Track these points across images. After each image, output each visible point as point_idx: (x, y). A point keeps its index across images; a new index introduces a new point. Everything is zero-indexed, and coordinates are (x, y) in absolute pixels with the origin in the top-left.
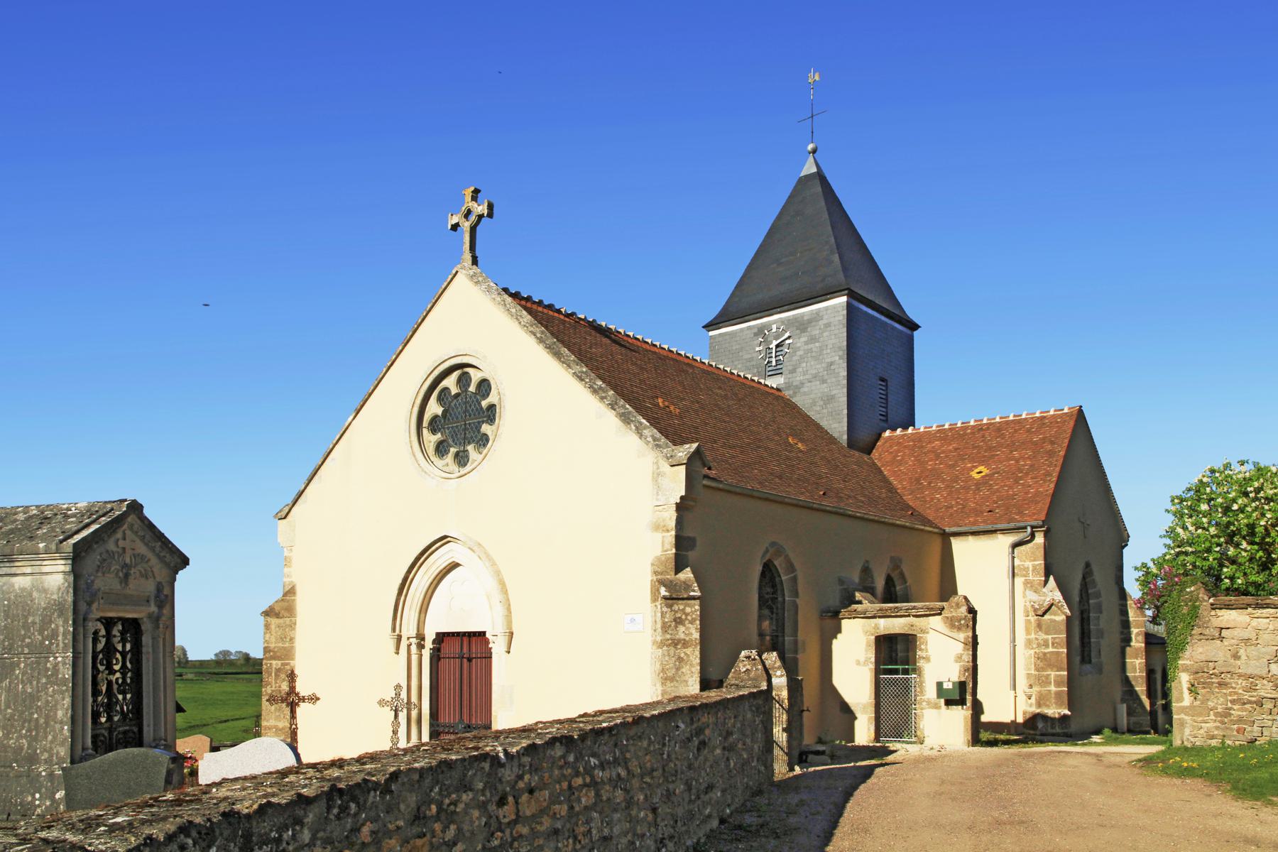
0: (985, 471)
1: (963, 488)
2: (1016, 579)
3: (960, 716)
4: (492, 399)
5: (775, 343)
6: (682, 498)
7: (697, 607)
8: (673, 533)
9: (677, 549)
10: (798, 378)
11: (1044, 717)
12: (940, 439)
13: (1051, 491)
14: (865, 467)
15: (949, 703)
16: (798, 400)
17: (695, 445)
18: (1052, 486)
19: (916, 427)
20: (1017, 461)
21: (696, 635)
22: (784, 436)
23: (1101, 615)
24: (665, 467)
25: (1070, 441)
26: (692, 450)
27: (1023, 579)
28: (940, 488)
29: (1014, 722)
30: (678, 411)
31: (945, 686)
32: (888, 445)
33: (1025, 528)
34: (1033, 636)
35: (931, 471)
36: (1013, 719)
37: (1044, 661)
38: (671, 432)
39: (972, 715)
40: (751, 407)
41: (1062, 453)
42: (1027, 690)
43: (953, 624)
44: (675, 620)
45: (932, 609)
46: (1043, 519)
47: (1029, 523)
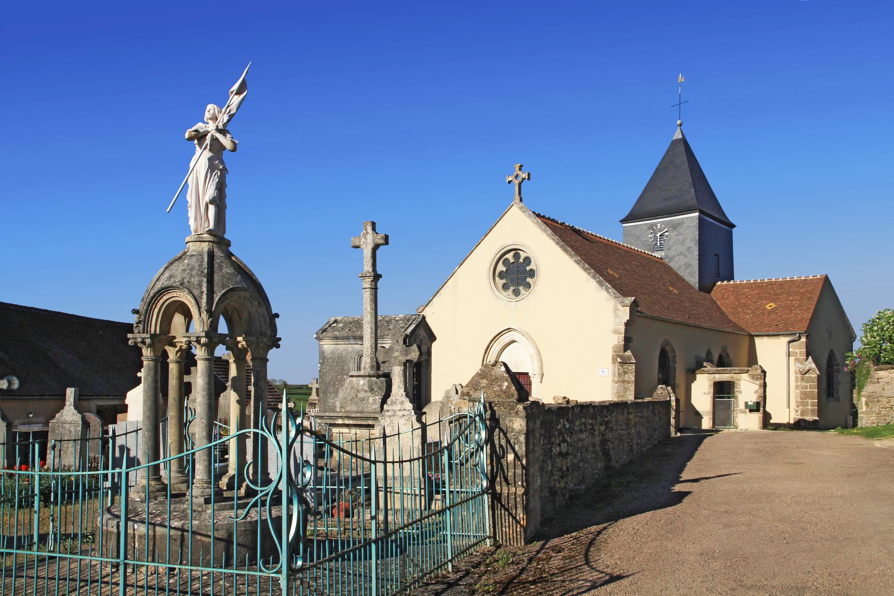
0: (774, 305)
1: (761, 313)
2: (790, 358)
3: (757, 417)
4: (532, 266)
5: (659, 234)
6: (627, 320)
7: (634, 367)
8: (623, 335)
9: (625, 342)
10: (672, 254)
11: (804, 421)
12: (748, 288)
13: (810, 317)
14: (708, 301)
15: (751, 411)
16: (672, 265)
17: (633, 298)
18: (810, 315)
19: (735, 281)
20: (792, 301)
21: (633, 379)
22: (667, 286)
23: (839, 375)
24: (620, 307)
25: (820, 292)
26: (632, 300)
27: (794, 358)
28: (748, 313)
29: (788, 424)
30: (618, 275)
31: (749, 404)
32: (719, 289)
33: (796, 334)
34: (799, 384)
35: (743, 304)
36: (788, 421)
37: (805, 395)
38: (620, 288)
39: (763, 416)
40: (650, 271)
41: (816, 299)
42: (796, 408)
43: (754, 377)
44: (624, 372)
45: (743, 371)
46: (805, 330)
47: (797, 332)
